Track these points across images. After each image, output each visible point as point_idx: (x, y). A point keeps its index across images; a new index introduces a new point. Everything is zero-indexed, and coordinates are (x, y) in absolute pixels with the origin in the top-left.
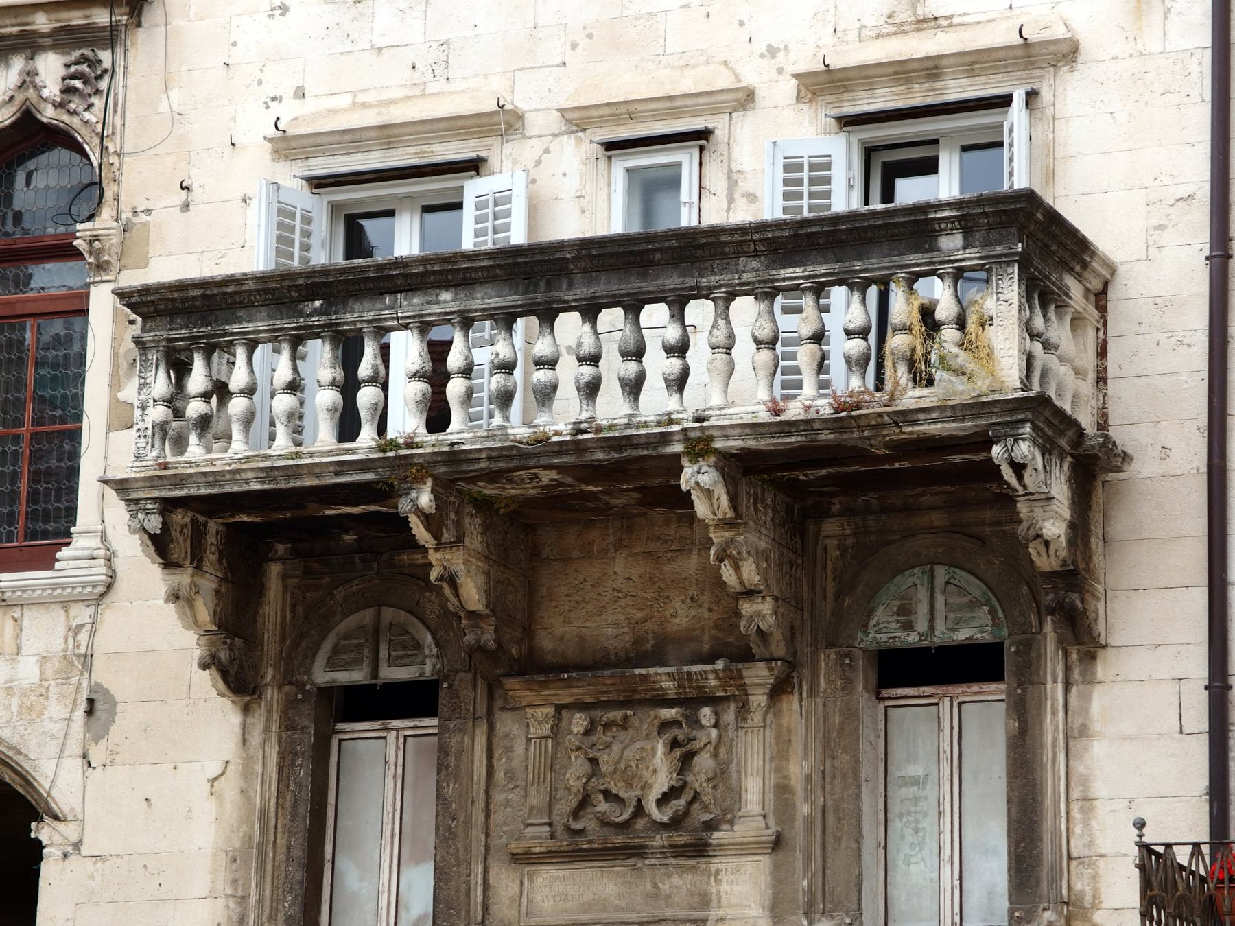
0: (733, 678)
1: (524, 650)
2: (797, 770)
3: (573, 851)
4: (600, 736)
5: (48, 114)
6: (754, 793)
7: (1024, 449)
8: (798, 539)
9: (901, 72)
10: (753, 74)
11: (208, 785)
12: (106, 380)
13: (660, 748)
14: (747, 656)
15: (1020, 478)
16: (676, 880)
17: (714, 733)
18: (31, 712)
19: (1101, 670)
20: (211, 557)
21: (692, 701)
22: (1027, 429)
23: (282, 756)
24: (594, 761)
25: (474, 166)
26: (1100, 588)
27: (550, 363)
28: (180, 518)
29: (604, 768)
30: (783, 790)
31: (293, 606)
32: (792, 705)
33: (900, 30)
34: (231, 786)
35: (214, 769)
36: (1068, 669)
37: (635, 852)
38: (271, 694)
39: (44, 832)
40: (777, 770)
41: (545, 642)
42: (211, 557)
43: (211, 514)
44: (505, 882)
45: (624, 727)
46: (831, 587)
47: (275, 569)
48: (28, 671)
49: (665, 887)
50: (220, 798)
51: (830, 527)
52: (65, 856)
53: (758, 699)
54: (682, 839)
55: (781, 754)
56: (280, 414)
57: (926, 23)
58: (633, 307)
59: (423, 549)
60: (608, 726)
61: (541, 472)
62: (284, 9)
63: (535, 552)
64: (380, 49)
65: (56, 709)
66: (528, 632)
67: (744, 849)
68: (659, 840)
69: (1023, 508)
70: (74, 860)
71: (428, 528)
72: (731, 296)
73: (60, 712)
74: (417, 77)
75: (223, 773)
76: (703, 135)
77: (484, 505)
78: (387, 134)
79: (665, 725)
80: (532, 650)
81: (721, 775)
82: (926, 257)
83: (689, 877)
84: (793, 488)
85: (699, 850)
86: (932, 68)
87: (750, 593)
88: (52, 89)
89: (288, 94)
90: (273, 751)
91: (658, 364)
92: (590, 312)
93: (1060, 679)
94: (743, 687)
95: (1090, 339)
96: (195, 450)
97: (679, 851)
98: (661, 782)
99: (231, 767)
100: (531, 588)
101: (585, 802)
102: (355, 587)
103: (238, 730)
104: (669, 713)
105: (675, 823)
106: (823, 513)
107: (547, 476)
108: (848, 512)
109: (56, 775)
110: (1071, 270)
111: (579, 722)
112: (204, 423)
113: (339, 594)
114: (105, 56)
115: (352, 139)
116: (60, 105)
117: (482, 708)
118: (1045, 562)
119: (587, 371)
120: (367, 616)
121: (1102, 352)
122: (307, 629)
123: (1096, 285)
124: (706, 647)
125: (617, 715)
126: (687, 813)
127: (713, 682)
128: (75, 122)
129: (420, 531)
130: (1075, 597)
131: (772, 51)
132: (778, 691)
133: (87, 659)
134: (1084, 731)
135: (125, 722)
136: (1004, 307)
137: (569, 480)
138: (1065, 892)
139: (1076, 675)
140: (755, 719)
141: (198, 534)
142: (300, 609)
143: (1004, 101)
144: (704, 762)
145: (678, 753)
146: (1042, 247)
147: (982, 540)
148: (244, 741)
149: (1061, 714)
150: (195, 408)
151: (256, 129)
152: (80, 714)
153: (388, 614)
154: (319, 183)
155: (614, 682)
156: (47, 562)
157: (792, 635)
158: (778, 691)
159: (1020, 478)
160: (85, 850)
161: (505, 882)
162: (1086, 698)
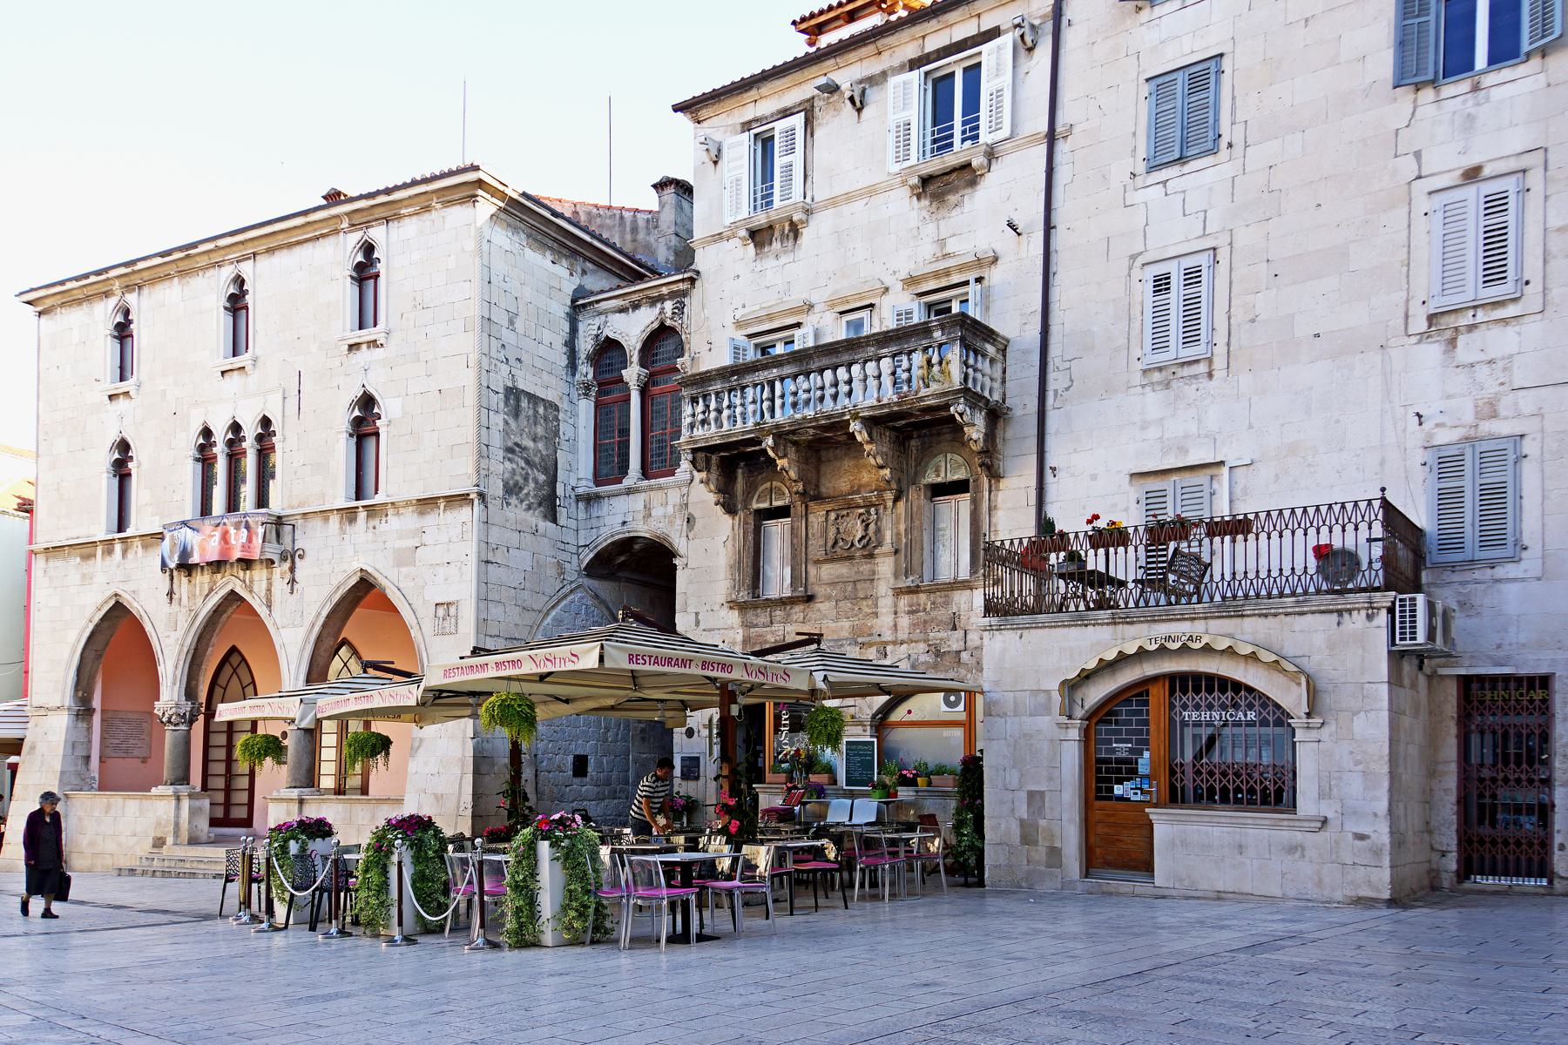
0: (880, 496)
2: (902, 527)
5: (668, 323)
6: (888, 536)
9: (937, 275)
10: (889, 281)
18: (671, 523)
20: (714, 468)
21: (868, 506)
25: (798, 325)
28: (700, 455)
32: (901, 505)
34: (729, 543)
37: (851, 558)
38: (741, 514)
39: (677, 561)
41: (823, 490)
42: (714, 468)
44: (812, 570)
48: (670, 509)
51: (913, 443)
56: (738, 416)
57: (946, 256)
58: (835, 368)
63: (819, 460)
65: (679, 522)
66: (817, 486)
67: (885, 555)
72: (866, 362)
73: (680, 522)
76: (872, 305)
77: (795, 443)
78: (770, 317)
81: (878, 531)
84: (894, 429)
85: (871, 556)
86: (947, 273)
88: (669, 314)
91: (844, 388)
92: (821, 371)
95: (999, 367)
97: (865, 557)
98: (859, 535)
100: (818, 472)
101: (836, 543)
106: (911, 437)
107: (811, 431)
109: (679, 543)
111: (833, 516)
112: (703, 422)
115: (759, 320)
120: (768, 485)
121: (1004, 372)
122: (751, 489)
129: (771, 453)
132: (896, 500)
135: (698, 525)
141: (708, 461)
143: (967, 283)
144: (872, 527)
146: (975, 335)
150: (701, 417)
154: (750, 336)
156: (673, 474)
157: (899, 481)
158: (896, 500)
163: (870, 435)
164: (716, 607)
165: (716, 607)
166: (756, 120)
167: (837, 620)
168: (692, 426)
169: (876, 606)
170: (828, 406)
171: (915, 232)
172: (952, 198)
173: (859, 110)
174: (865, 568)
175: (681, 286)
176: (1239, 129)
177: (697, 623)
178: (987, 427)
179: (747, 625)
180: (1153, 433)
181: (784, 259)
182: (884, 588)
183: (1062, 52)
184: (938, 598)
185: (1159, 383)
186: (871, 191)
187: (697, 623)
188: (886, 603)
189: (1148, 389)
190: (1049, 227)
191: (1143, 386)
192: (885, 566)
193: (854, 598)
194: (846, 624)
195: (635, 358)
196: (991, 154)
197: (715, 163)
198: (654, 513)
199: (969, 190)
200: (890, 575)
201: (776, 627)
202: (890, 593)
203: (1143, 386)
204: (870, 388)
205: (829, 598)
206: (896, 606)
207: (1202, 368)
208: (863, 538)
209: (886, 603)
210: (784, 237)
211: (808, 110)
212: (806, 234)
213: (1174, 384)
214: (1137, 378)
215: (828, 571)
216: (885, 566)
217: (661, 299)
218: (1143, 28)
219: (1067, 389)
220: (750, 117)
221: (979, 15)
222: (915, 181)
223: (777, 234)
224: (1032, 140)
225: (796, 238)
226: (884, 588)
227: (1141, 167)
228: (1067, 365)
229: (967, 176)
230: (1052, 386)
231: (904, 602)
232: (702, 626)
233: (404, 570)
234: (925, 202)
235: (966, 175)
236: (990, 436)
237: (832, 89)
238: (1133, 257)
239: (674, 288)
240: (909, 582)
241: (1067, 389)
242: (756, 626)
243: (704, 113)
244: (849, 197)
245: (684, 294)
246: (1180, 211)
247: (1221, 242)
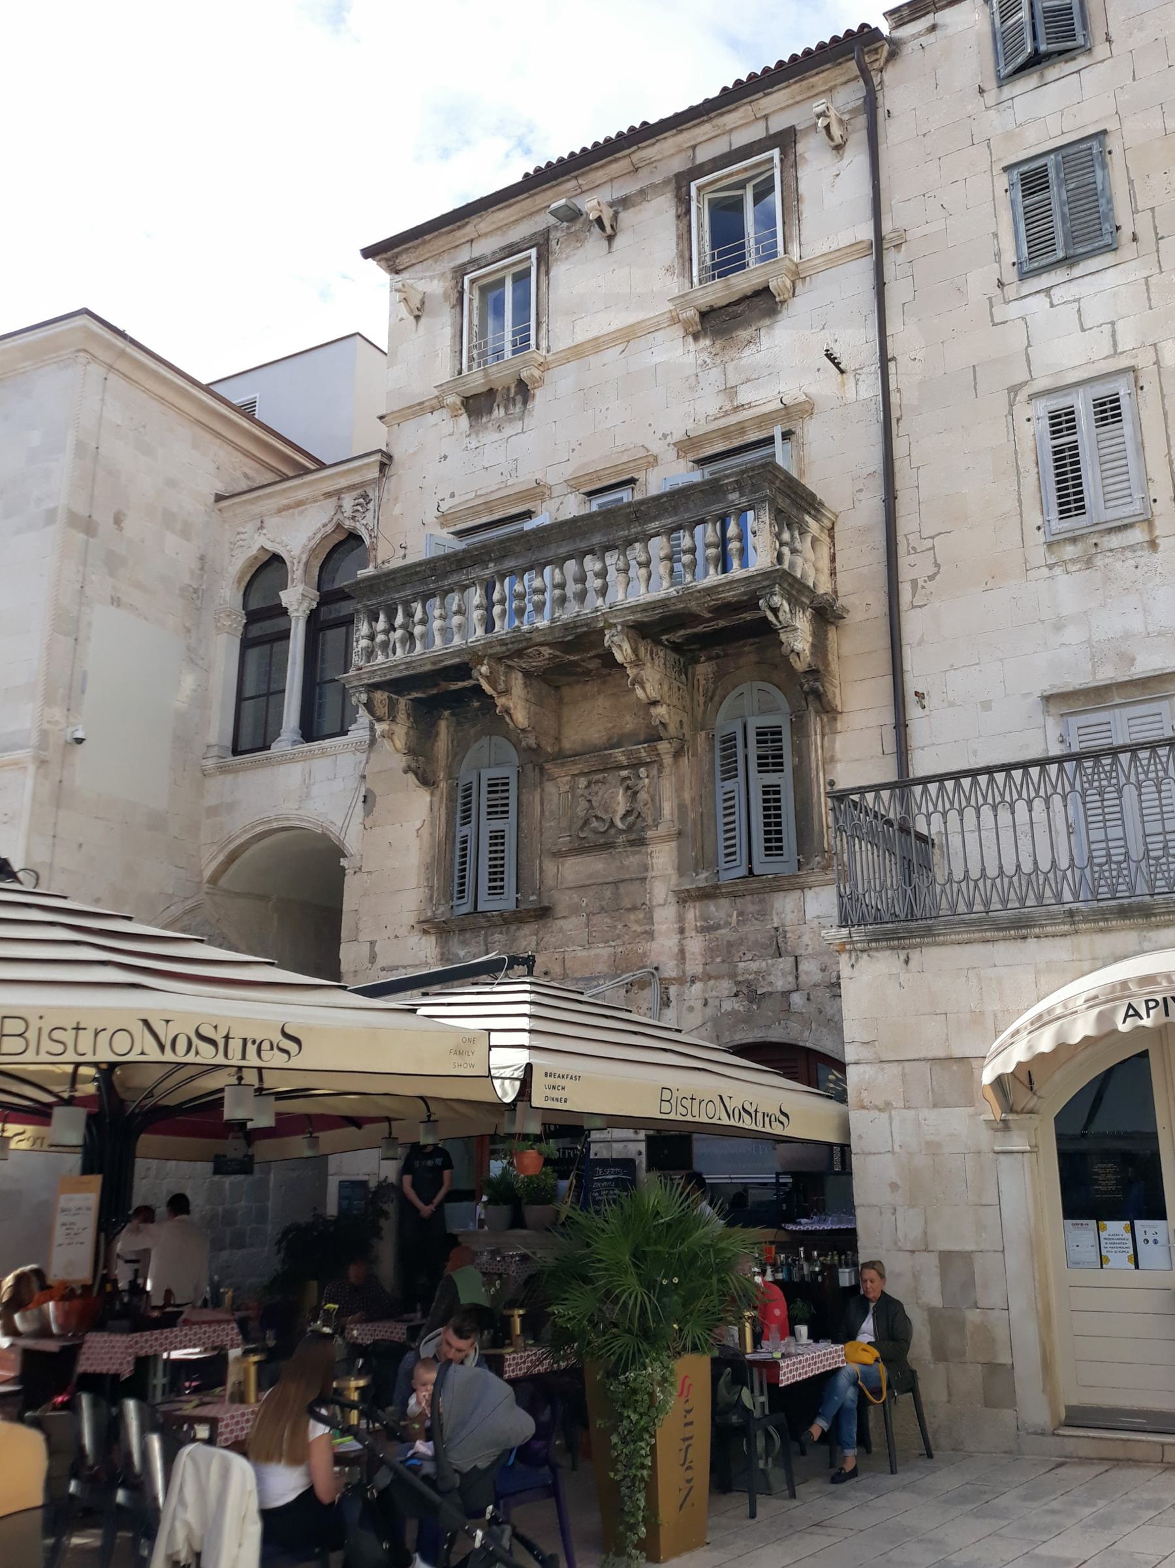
1: (556, 749)
2: (687, 796)
3: (582, 849)
4: (594, 788)
6: (667, 808)
7: (777, 600)
8: (683, 676)
9: (725, 433)
10: (656, 447)
13: (621, 792)
14: (661, 739)
15: (777, 617)
16: (631, 859)
17: (647, 780)
19: (839, 725)
20: (402, 716)
21: (635, 766)
22: (777, 588)
24: (590, 801)
26: (837, 682)
27: (542, 591)
29: (594, 804)
30: (682, 808)
32: (684, 761)
33: (726, 414)
34: (425, 833)
35: (418, 824)
36: (823, 727)
37: (609, 846)
40: (678, 797)
43: (399, 693)
44: (550, 867)
45: (603, 783)
46: (702, 700)
47: (443, 724)
49: (626, 863)
53: (668, 760)
54: (633, 836)
55: (679, 789)
59: (492, 697)
60: (597, 782)
61: (542, 649)
62: (445, 457)
66: (558, 739)
67: (663, 839)
68: (621, 839)
69: (783, 637)
71: (489, 684)
74: (504, 478)
76: (632, 481)
78: (488, 506)
79: (624, 779)
80: (560, 749)
82: (721, 505)
83: (637, 856)
85: (641, 842)
86: (741, 428)
87: (655, 703)
89: (447, 497)
90: (443, 811)
91: (594, 583)
93: (818, 731)
94: (658, 755)
95: (824, 551)
96: (380, 658)
97: (632, 843)
98: (621, 810)
100: (559, 717)
101: (586, 822)
104: (624, 773)
105: (630, 829)
106: (696, 661)
107: (546, 651)
108: (709, 659)
110: (809, 513)
111: (583, 782)
112: (385, 645)
115: (474, 511)
117: (538, 781)
118: (800, 666)
119: (557, 592)
121: (833, 559)
123: (828, 524)
124: (642, 738)
125: (600, 776)
126: (634, 824)
127: (644, 754)
130: (818, 684)
131: (665, 436)
134: (832, 760)
136: (762, 525)
137: (558, 653)
138: (826, 846)
139: (827, 730)
140: (667, 771)
141: (392, 705)
144: (643, 796)
145: (629, 792)
146: (794, 503)
147: (776, 666)
149: (820, 751)
150: (380, 638)
151: (431, 515)
155: (598, 762)
158: (677, 754)
159: (777, 617)
161: (550, 867)
162: (833, 741)
163: (635, 651)
166: (472, 261)
167: (589, 944)
168: (370, 654)
169: (650, 920)
170: (572, 610)
171: (693, 380)
172: (743, 334)
173: (610, 239)
174: (633, 861)
176: (1144, 220)
178: (815, 634)
180: (1073, 635)
181: (509, 430)
182: (661, 891)
183: (882, 148)
184: (749, 905)
185: (1074, 561)
186: (627, 335)
188: (665, 916)
189: (1058, 570)
190: (885, 360)
191: (1050, 567)
192: (663, 858)
193: (615, 909)
194: (603, 952)
196: (798, 276)
197: (417, 318)
199: (767, 322)
200: (671, 871)
202: (672, 899)
203: (1050, 567)
204: (636, 583)
205: (575, 910)
206: (681, 919)
207: (1138, 535)
208: (628, 813)
209: (665, 916)
210: (509, 401)
211: (542, 244)
212: (540, 398)
213: (1099, 561)
214: (1038, 554)
215: (574, 869)
216: (663, 858)
218: (992, 112)
219: (931, 578)
220: (466, 259)
221: (766, 117)
222: (691, 314)
223: (499, 399)
224: (851, 251)
225: (525, 402)
226: (661, 891)
227: (1011, 275)
228: (928, 543)
229: (761, 303)
230: (906, 572)
231: (692, 914)
234: (705, 342)
235: (763, 303)
236: (820, 646)
237: (572, 215)
238: (1014, 390)
240: (702, 879)
241: (931, 578)
243: (404, 260)
244: (597, 345)
246: (1078, 325)
247: (1144, 361)
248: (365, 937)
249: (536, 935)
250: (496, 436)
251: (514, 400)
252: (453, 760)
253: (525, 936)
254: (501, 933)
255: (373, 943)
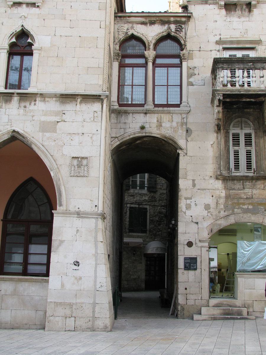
5: (173, 34)
11: (211, 146)
12: (186, 78)
23: (225, 141)
31: (225, 117)
34: (215, 146)
35: (212, 143)
39: (179, 151)
48: (174, 124)
50: (213, 148)
52: (184, 156)
62: (216, 21)
64: (234, 29)
70: (186, 156)
75: (213, 144)
78: (238, 42)
88: (173, 30)
89: (218, 35)
99: (215, 142)
102: (237, 114)
103: (216, 136)
109: (181, 142)
113: (234, 115)
114: (183, 26)
116: (176, 33)
120: (239, 119)
128: (178, 35)
133: (186, 124)
142: (227, 117)
148: (217, 139)
152: (185, 132)
153: (243, 119)
160: (188, 155)
164: (207, 178)
165: (207, 178)
175: (183, 19)
177: (194, 185)
179: (226, 188)
187: (194, 185)
195: (152, 47)
198: (163, 125)
201: (246, 190)
212: (255, 11)
217: (169, 23)
232: (197, 187)
233: (48, 135)
239: (178, 19)
242: (234, 189)
245: (184, 23)
248: (190, 177)
249: (264, 184)
250: (238, 19)
251: (245, 10)
252: (226, 123)
253: (259, 184)
254: (249, 182)
255: (194, 180)
